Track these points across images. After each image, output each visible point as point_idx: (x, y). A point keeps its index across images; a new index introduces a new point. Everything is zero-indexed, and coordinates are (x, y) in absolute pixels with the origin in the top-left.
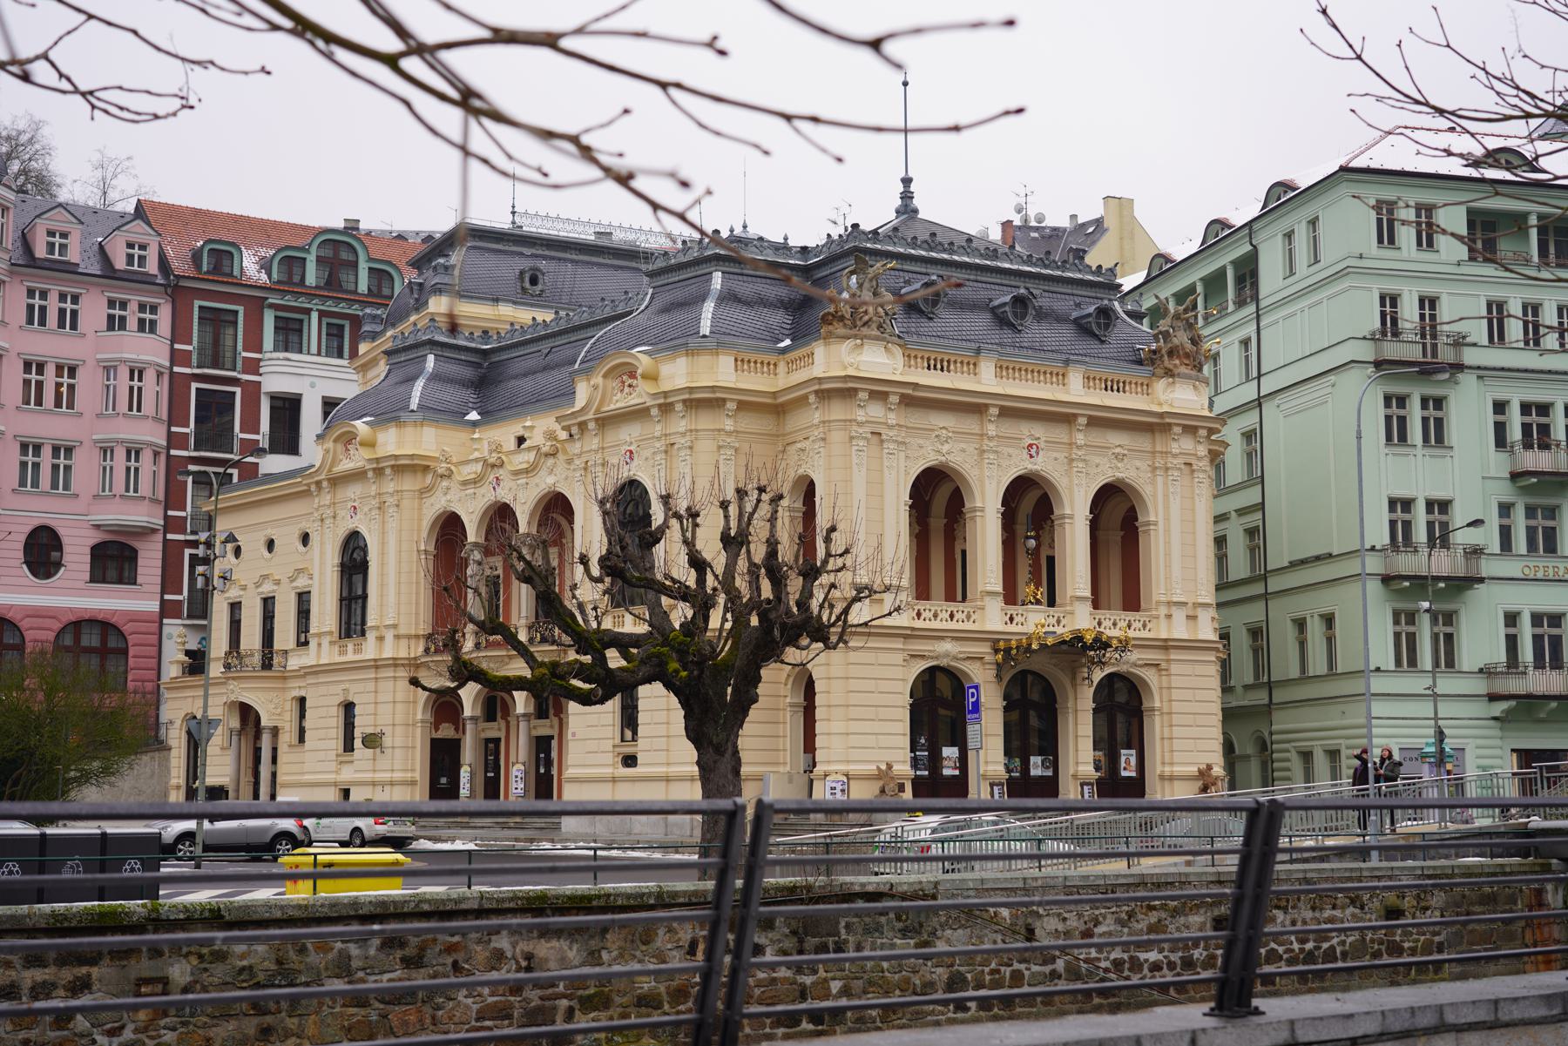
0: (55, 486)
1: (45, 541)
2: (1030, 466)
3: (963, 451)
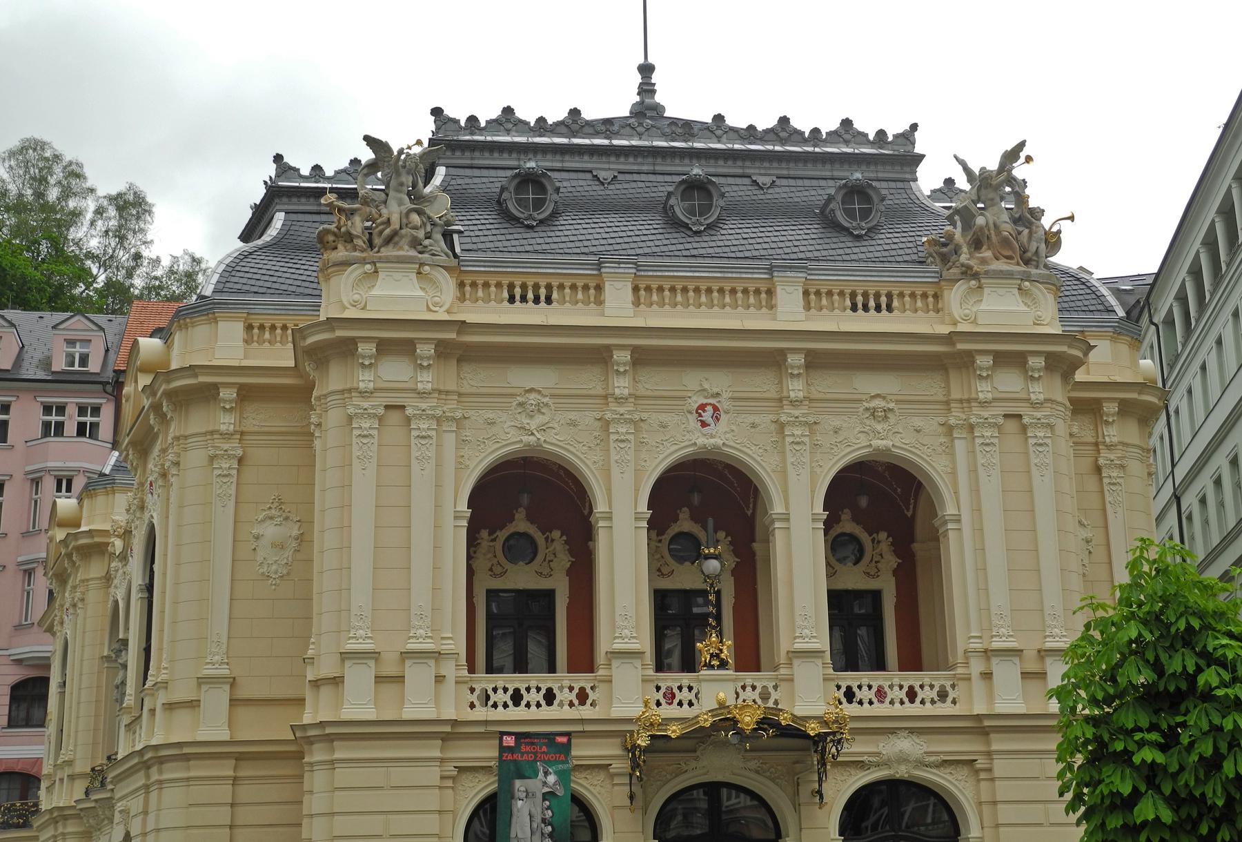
2: (701, 441)
3: (573, 424)
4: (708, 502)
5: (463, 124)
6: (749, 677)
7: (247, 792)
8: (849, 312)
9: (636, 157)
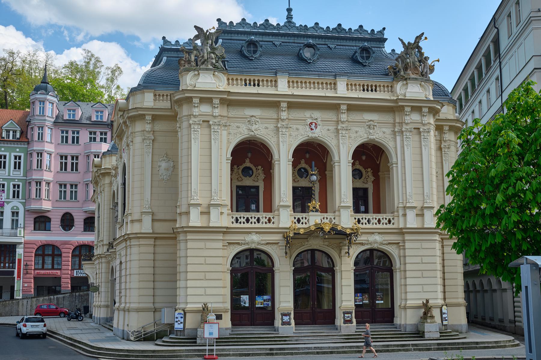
0: (71, 198)
1: (69, 218)
2: (310, 135)
3: (266, 128)
4: (312, 156)
5: (228, 24)
6: (325, 215)
7: (159, 250)
8: (362, 91)
9: (288, 37)
